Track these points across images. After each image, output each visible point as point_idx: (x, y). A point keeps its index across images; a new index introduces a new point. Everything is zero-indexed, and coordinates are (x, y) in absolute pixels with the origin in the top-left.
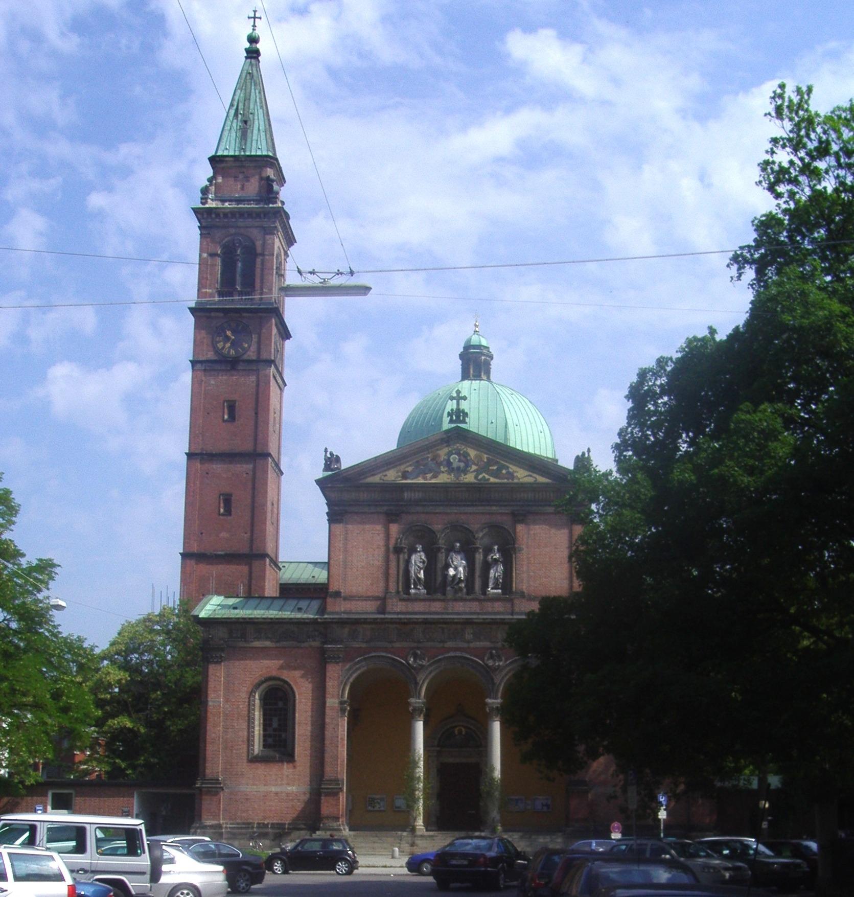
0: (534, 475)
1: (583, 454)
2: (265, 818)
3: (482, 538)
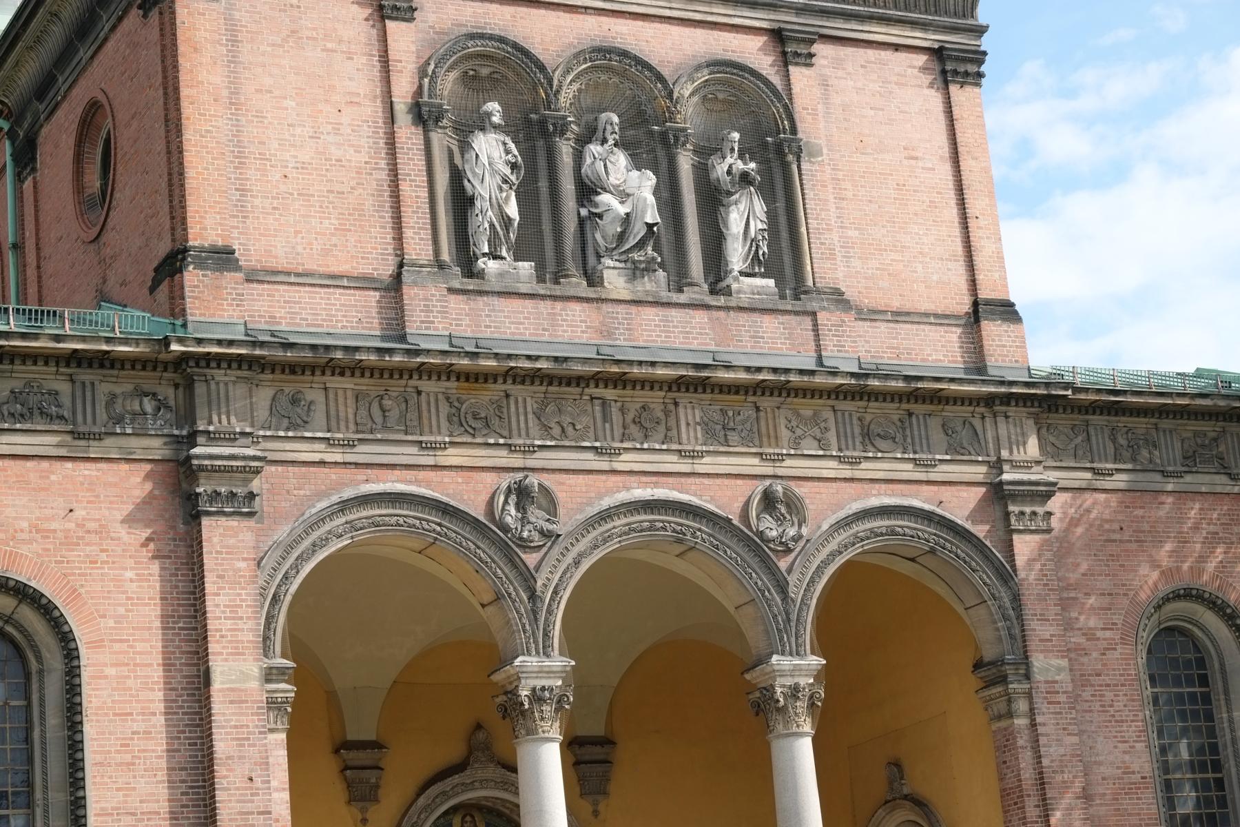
3: (690, 114)
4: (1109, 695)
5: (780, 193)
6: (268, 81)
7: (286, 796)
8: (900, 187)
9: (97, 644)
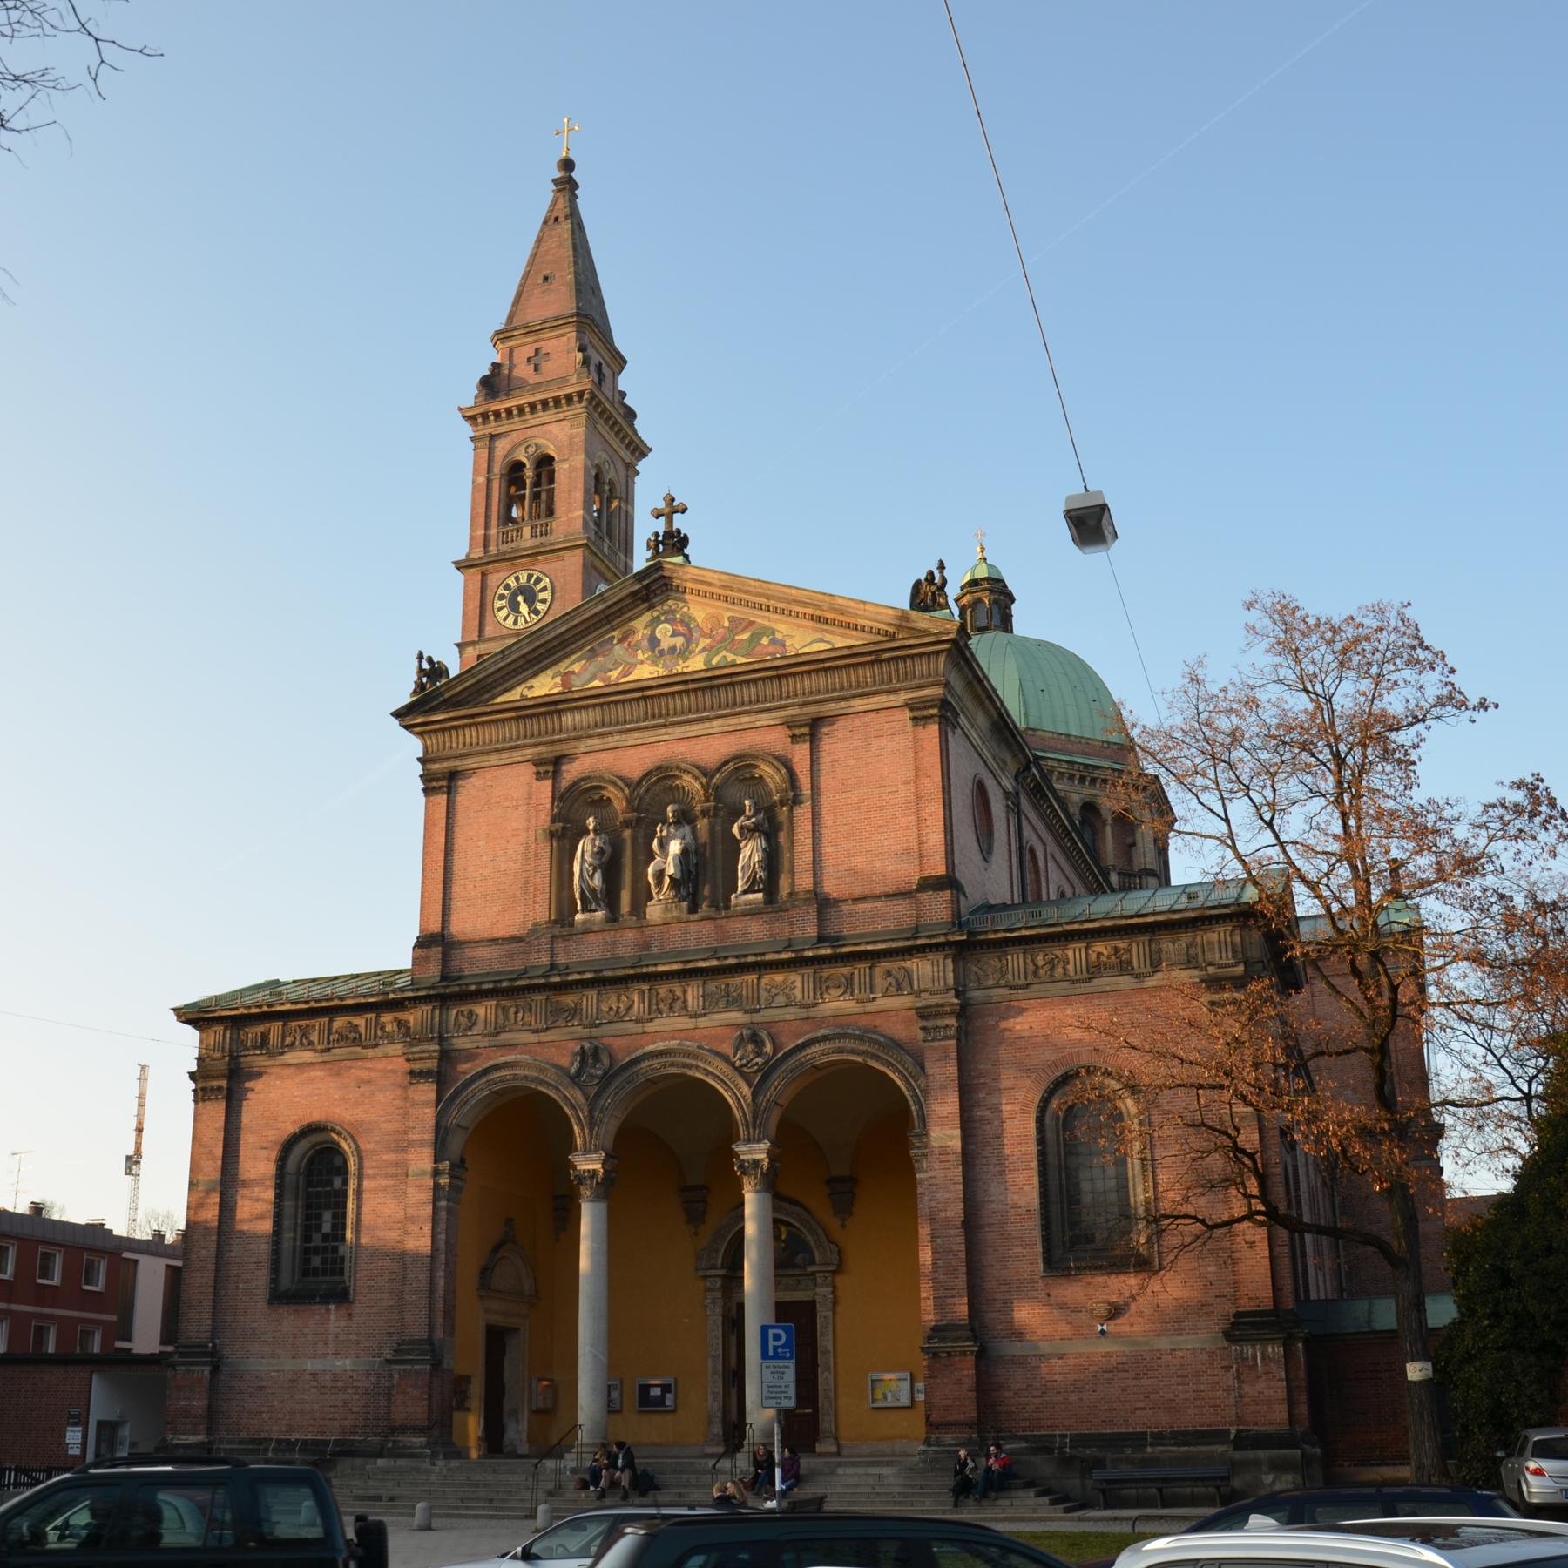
0: (828, 637)
2: (291, 1429)
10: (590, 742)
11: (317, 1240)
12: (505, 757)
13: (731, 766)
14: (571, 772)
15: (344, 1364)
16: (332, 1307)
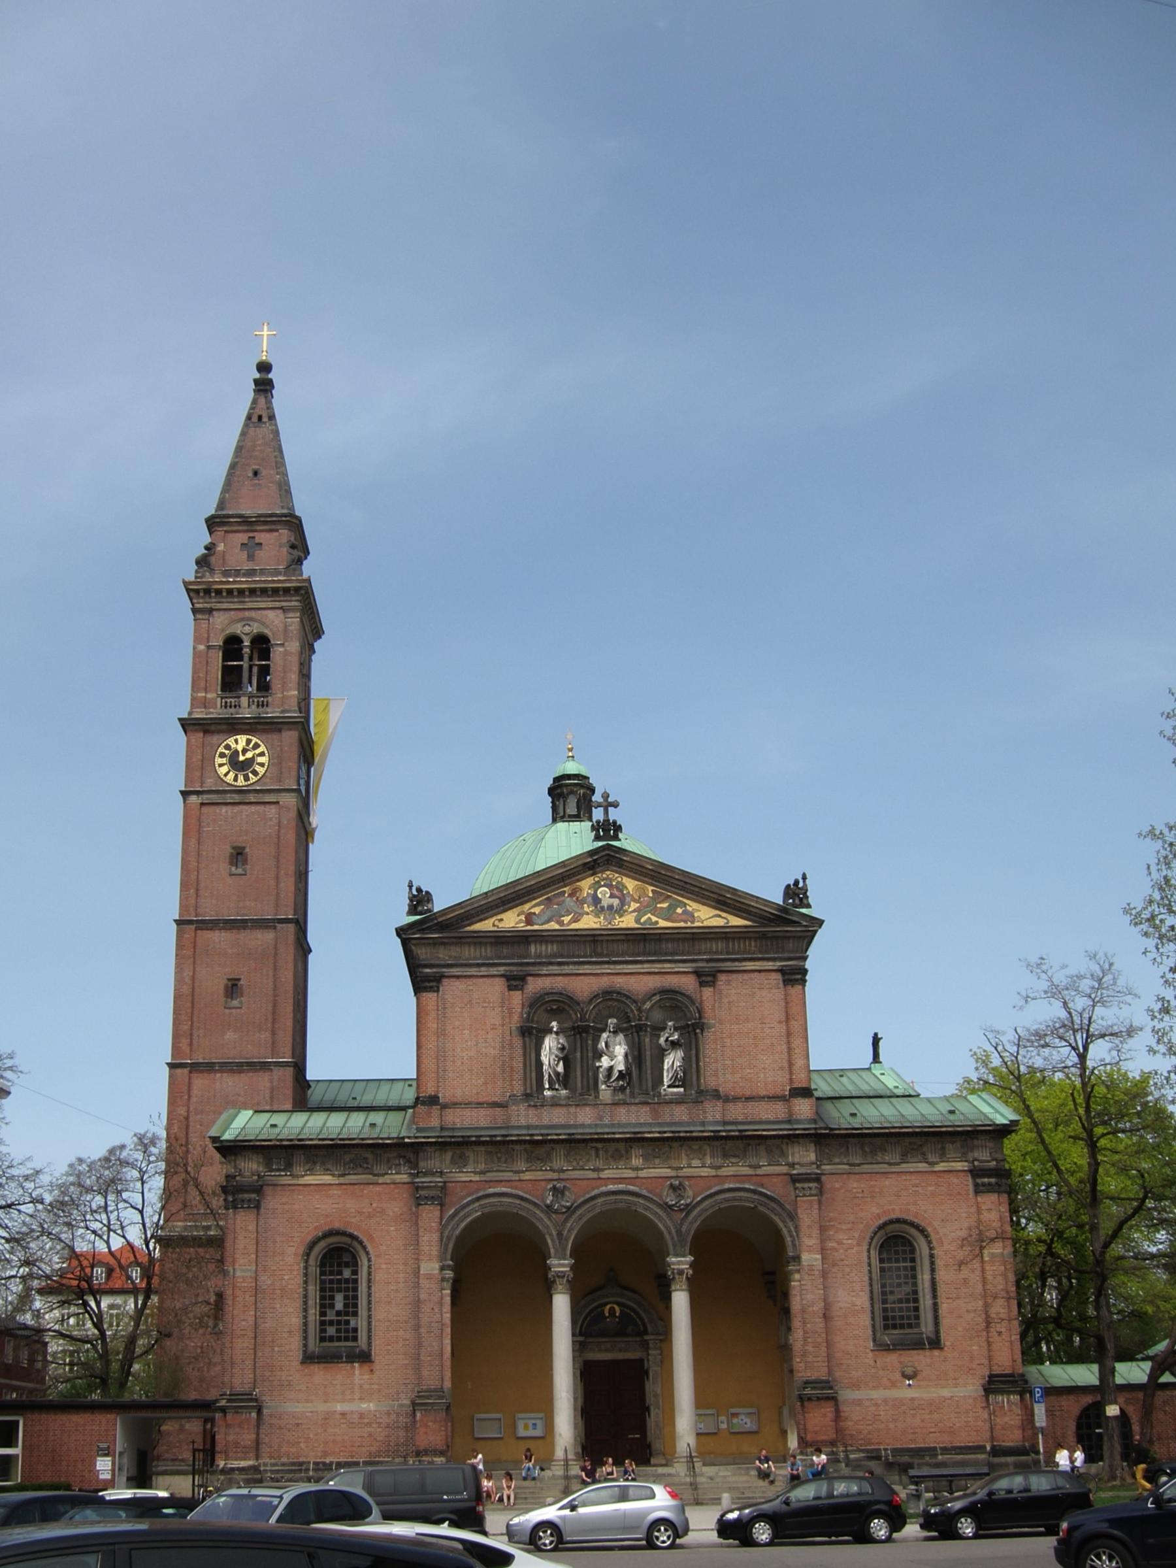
0: (724, 915)
1: (796, 883)
2: (325, 1454)
4: (847, 1270)
5: (694, 1047)
6: (457, 1023)
7: (449, 1315)
8: (755, 1038)
9: (378, 1256)
10: (551, 968)
11: (331, 1316)
12: (484, 971)
13: (657, 998)
14: (534, 985)
15: (368, 1406)
16: (356, 1365)
